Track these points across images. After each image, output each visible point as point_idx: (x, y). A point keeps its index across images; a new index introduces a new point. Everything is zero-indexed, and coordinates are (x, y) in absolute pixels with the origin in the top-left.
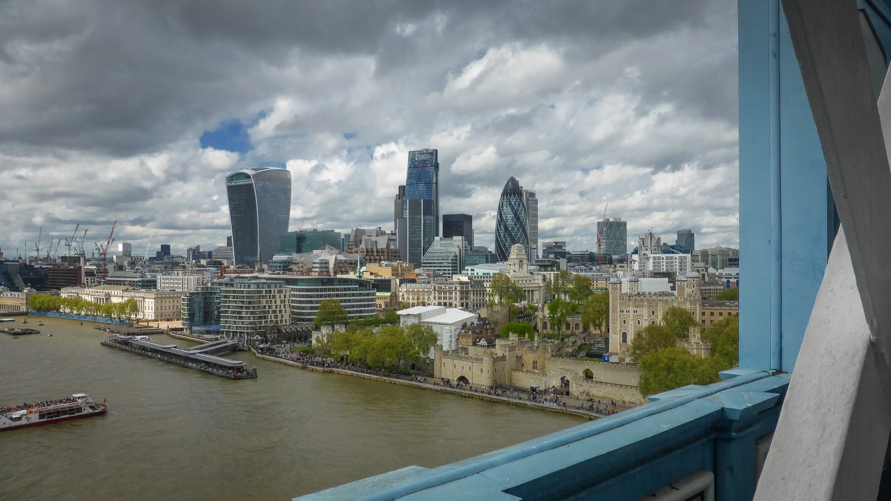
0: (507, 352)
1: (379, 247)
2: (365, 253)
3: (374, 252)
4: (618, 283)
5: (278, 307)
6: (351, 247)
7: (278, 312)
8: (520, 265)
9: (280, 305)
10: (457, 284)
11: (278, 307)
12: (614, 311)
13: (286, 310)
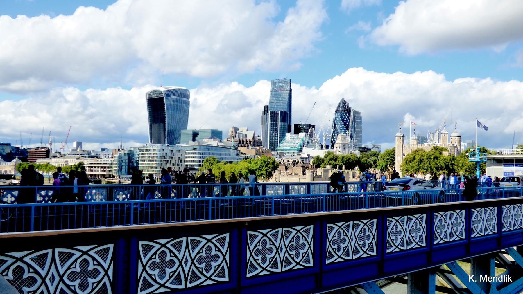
0: (323, 173)
1: (248, 138)
2: (238, 142)
3: (243, 141)
4: (401, 136)
5: (177, 161)
6: (229, 139)
7: (177, 165)
8: (344, 148)
9: (178, 161)
10: (299, 158)
11: (177, 161)
13: (182, 164)
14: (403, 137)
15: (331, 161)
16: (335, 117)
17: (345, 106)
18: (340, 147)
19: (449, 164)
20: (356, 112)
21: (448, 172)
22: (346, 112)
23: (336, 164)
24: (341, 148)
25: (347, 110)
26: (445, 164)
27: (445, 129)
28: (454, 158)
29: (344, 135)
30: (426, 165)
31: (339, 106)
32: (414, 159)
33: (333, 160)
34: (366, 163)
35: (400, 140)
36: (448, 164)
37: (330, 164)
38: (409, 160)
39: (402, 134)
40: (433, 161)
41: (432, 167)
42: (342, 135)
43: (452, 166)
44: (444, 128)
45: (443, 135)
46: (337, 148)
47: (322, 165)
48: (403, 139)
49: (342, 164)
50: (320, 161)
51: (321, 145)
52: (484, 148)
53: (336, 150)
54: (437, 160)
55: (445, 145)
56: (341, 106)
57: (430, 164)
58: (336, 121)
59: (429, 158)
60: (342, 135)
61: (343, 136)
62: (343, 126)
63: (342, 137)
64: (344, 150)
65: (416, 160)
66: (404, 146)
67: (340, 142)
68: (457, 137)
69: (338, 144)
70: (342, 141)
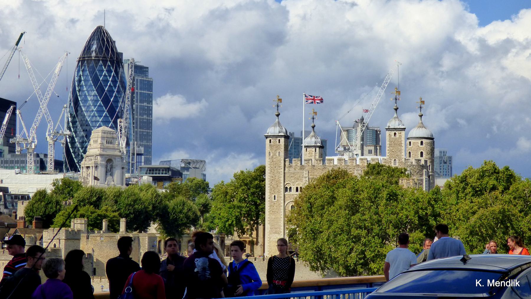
0: (63, 242)
8: (109, 168)
12: (273, 189)
14: (287, 137)
15: (84, 205)
16: (76, 79)
17: (107, 49)
18: (96, 167)
19: (426, 214)
21: (424, 235)
22: (109, 66)
23: (99, 215)
24: (100, 168)
25: (112, 62)
26: (417, 212)
28: (438, 198)
29: (110, 133)
30: (366, 217)
31: (88, 48)
32: (333, 199)
33: (91, 204)
34: (181, 212)
35: (278, 147)
36: (426, 214)
37: (82, 216)
38: (319, 202)
39: (284, 131)
40: (386, 205)
41: (384, 221)
42: (104, 132)
43: (435, 220)
44: (395, 115)
45: (393, 133)
46: (90, 170)
47: (59, 219)
48: (285, 145)
49: (116, 214)
50: (50, 206)
51: (38, 159)
52: (507, 169)
53: (85, 175)
54: (395, 203)
55: (397, 161)
56: (94, 47)
57: (377, 213)
58: (79, 91)
59: (375, 198)
60: (104, 132)
61: (105, 135)
62: (100, 106)
63: (103, 138)
64: (109, 173)
65: (338, 203)
66: (287, 163)
67: (97, 151)
68: (424, 141)
69: (92, 158)
70: (103, 148)
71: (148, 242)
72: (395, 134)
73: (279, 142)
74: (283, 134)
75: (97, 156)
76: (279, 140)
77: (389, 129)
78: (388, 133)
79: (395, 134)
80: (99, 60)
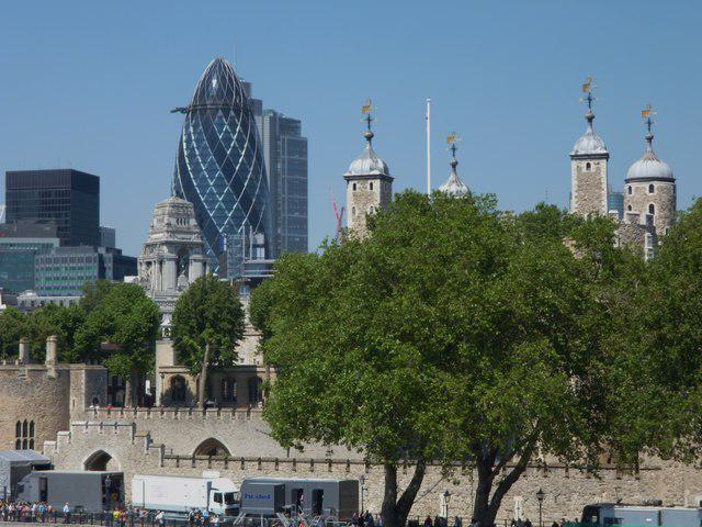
4: (374, 177)
16: (184, 138)
20: (281, 119)
25: (237, 112)
27: (593, 133)
39: (381, 165)
44: (589, 130)
48: (382, 193)
68: (656, 184)
71: (87, 382)
72: (588, 166)
73: (371, 188)
74: (376, 172)
75: (163, 244)
76: (371, 184)
77: (576, 157)
78: (574, 164)
79: (588, 166)
80: (217, 109)
